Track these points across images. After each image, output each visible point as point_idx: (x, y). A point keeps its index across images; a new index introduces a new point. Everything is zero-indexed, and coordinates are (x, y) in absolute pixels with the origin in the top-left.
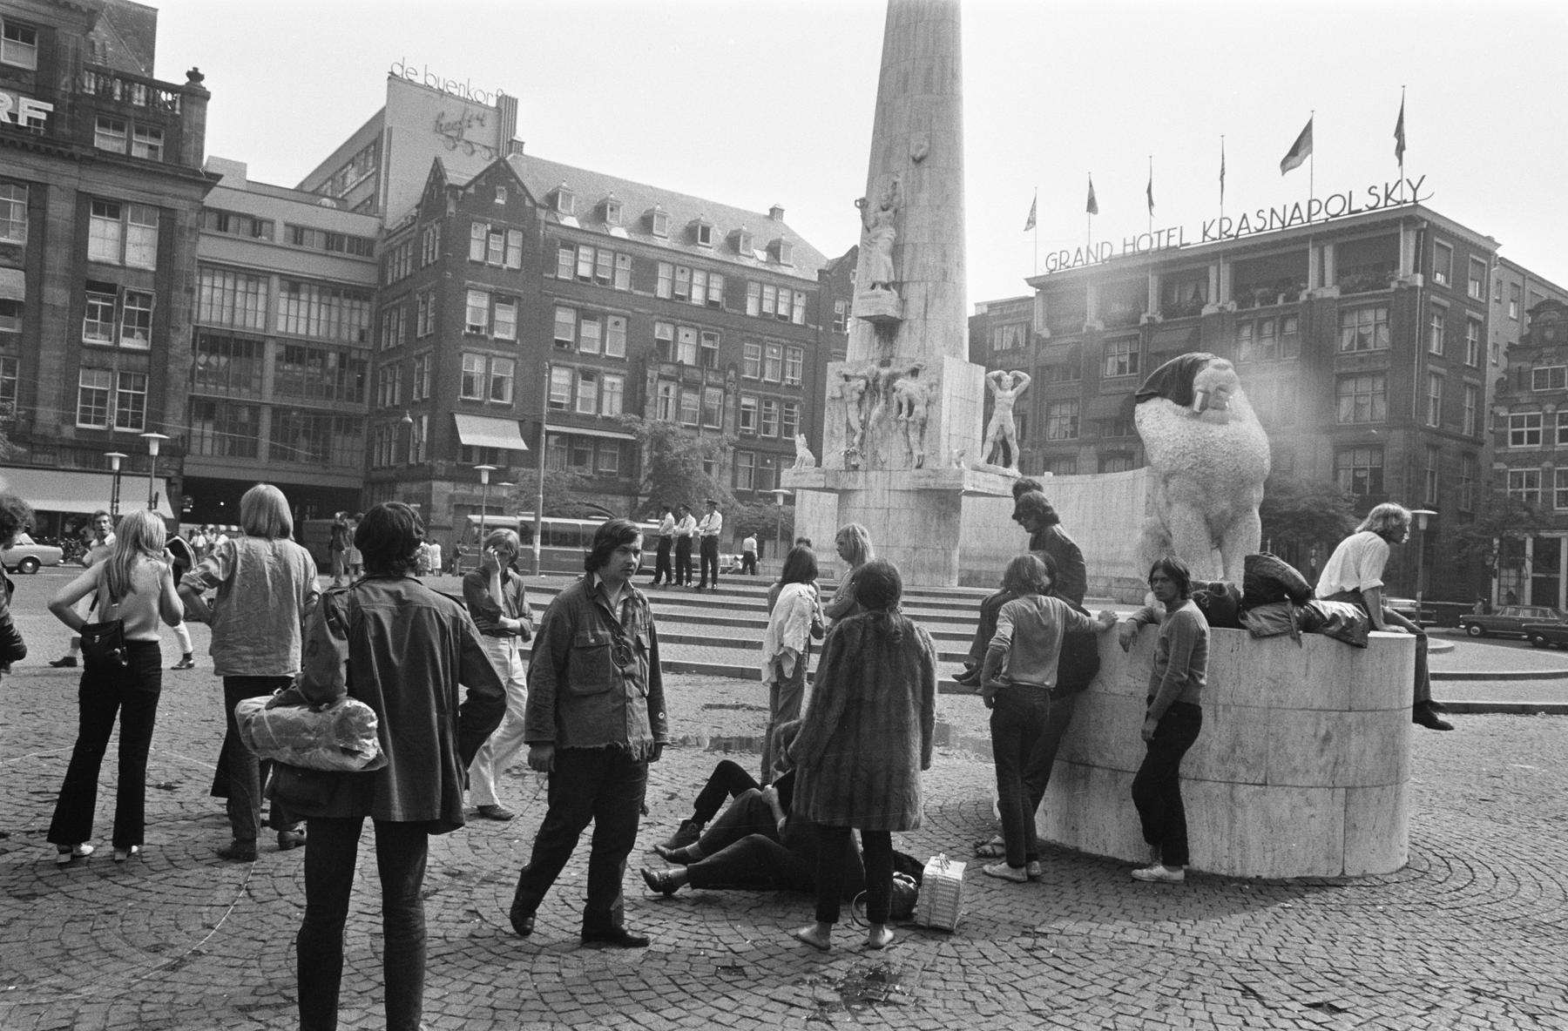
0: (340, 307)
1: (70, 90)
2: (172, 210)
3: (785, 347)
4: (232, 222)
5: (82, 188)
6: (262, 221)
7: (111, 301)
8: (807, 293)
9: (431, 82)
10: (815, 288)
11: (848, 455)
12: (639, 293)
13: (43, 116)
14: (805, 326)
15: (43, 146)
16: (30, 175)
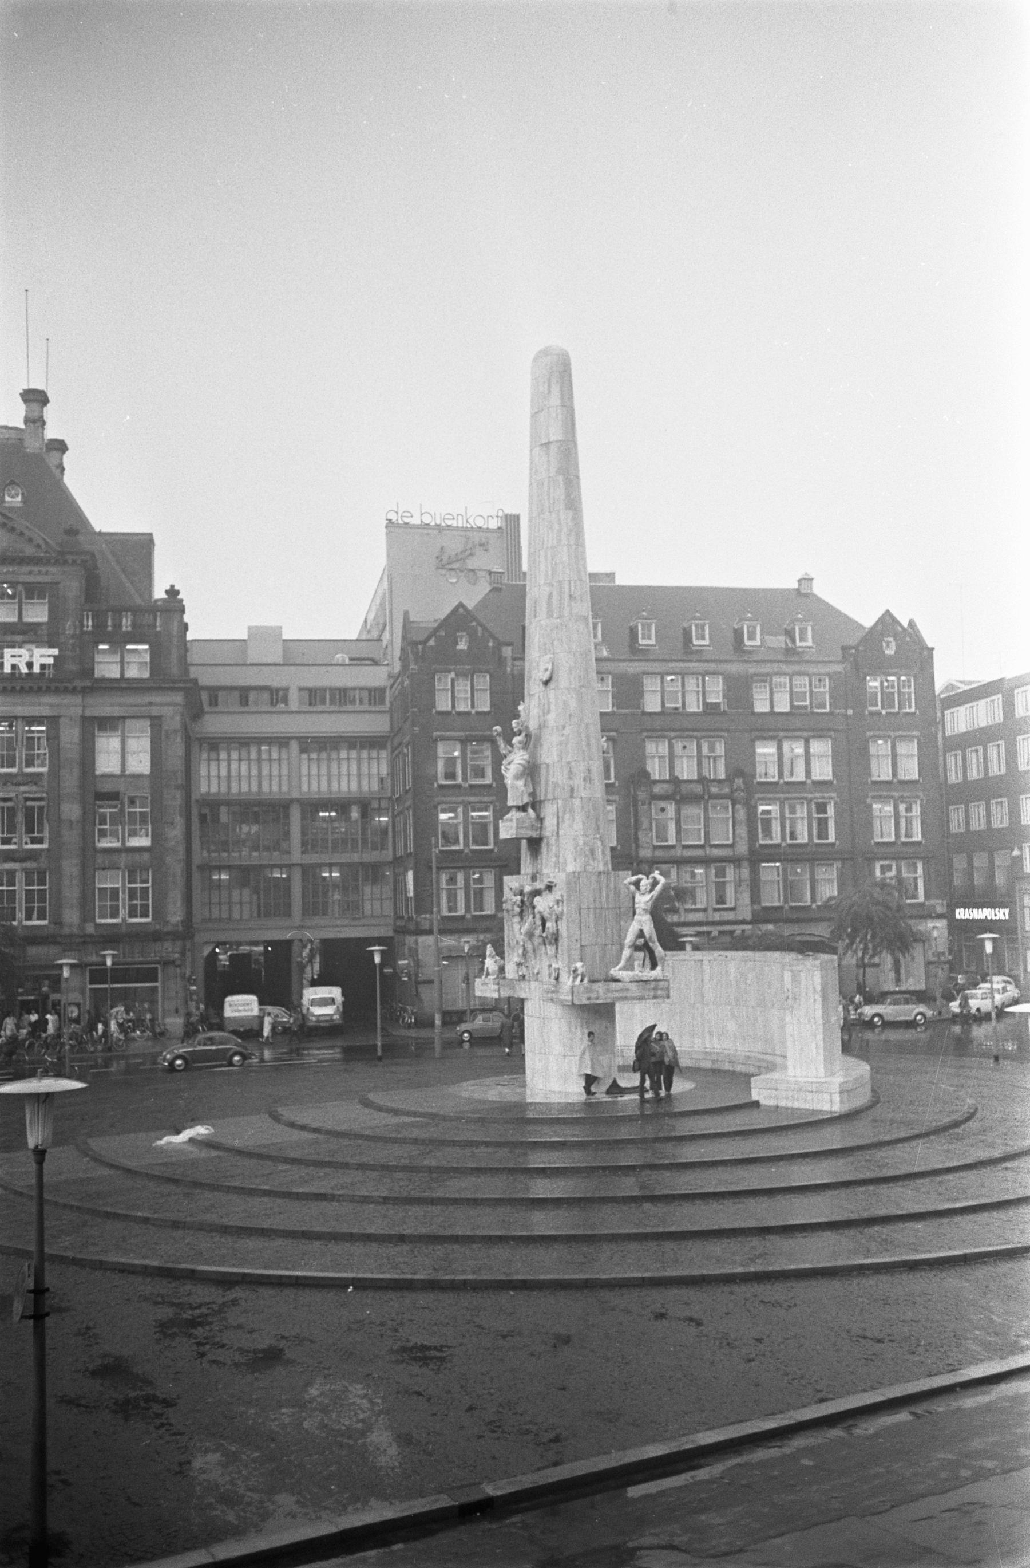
0: (359, 760)
1: (72, 632)
2: (159, 718)
3: (807, 741)
4: (252, 696)
5: (88, 713)
6: (277, 690)
7: (115, 807)
8: (828, 675)
9: (427, 520)
10: (839, 668)
11: (519, 964)
12: (624, 711)
13: (51, 661)
14: (831, 713)
15: (53, 686)
16: (46, 711)
